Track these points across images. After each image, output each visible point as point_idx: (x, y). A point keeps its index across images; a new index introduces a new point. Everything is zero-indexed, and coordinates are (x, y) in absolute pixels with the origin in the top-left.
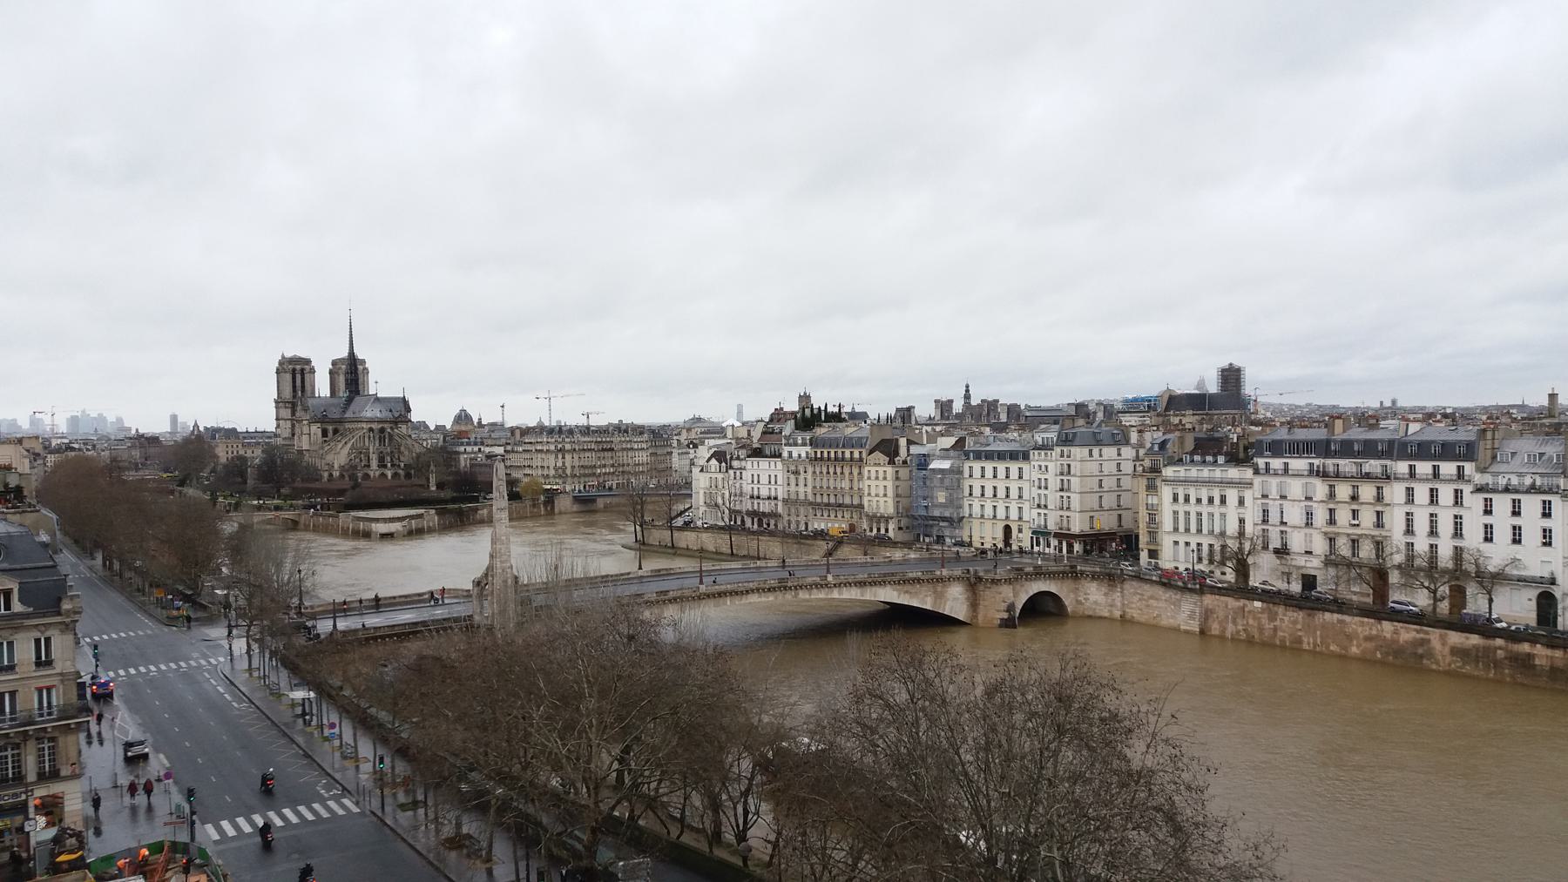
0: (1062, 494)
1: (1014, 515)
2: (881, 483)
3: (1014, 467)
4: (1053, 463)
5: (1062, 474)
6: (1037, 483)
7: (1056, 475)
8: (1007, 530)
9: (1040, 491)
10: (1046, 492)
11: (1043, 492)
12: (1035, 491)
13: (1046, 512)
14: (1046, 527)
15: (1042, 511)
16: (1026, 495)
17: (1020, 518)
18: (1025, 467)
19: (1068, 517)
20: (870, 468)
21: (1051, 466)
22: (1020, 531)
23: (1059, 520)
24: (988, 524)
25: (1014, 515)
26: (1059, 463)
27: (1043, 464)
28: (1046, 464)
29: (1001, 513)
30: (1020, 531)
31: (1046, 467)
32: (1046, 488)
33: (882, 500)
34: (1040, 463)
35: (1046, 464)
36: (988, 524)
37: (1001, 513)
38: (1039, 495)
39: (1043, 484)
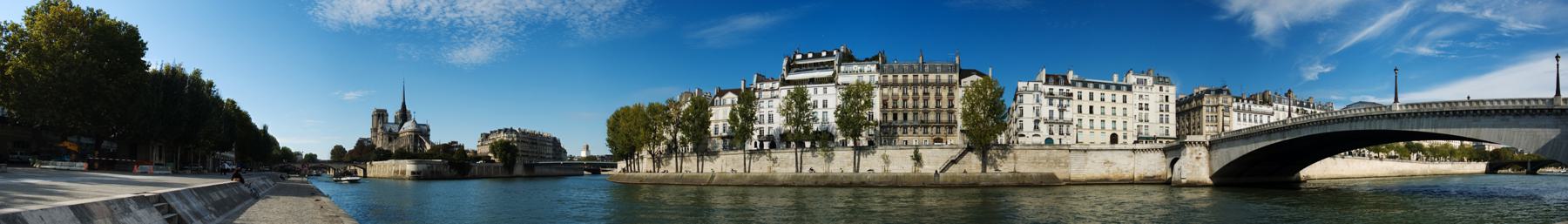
1: (1119, 126)
3: (1119, 95)
11: (1144, 112)
12: (1137, 111)
13: (1147, 124)
16: (1129, 112)
17: (1125, 129)
18: (1129, 95)
22: (1125, 137)
24: (1098, 133)
25: (1119, 126)
29: (1109, 125)
30: (1125, 137)
36: (1098, 133)
37: (1109, 125)
39: (1144, 106)
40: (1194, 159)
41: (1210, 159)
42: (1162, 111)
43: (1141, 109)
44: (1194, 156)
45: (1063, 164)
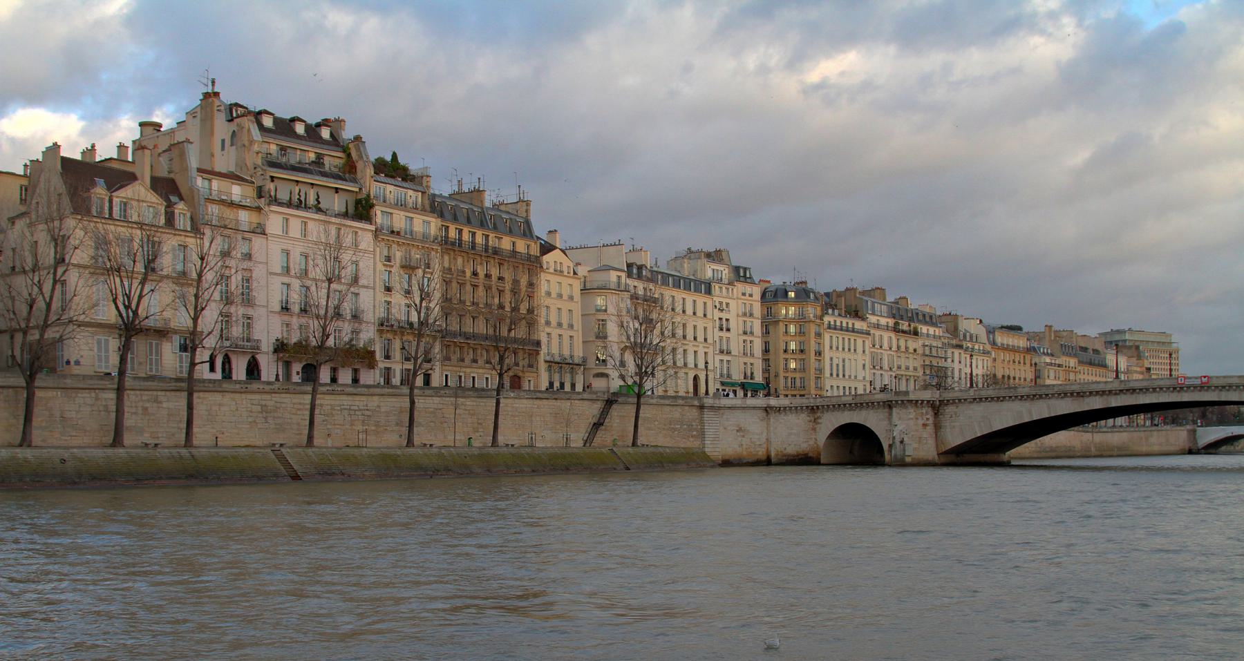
0: (745, 337)
2: (565, 306)
4: (735, 301)
5: (745, 314)
6: (718, 322)
7: (738, 315)
8: (696, 378)
9: (721, 334)
10: (728, 335)
11: (724, 334)
12: (718, 334)
13: (729, 358)
14: (729, 376)
15: (725, 358)
19: (752, 364)
20: (549, 277)
21: (733, 304)
23: (743, 366)
26: (740, 301)
27: (725, 301)
28: (728, 301)
31: (727, 304)
32: (728, 330)
33: (566, 334)
34: (721, 300)
35: (728, 301)
37: (691, 364)
38: (721, 338)
40: (921, 427)
41: (937, 427)
42: (745, 333)
43: (721, 329)
44: (921, 422)
45: (695, 433)
